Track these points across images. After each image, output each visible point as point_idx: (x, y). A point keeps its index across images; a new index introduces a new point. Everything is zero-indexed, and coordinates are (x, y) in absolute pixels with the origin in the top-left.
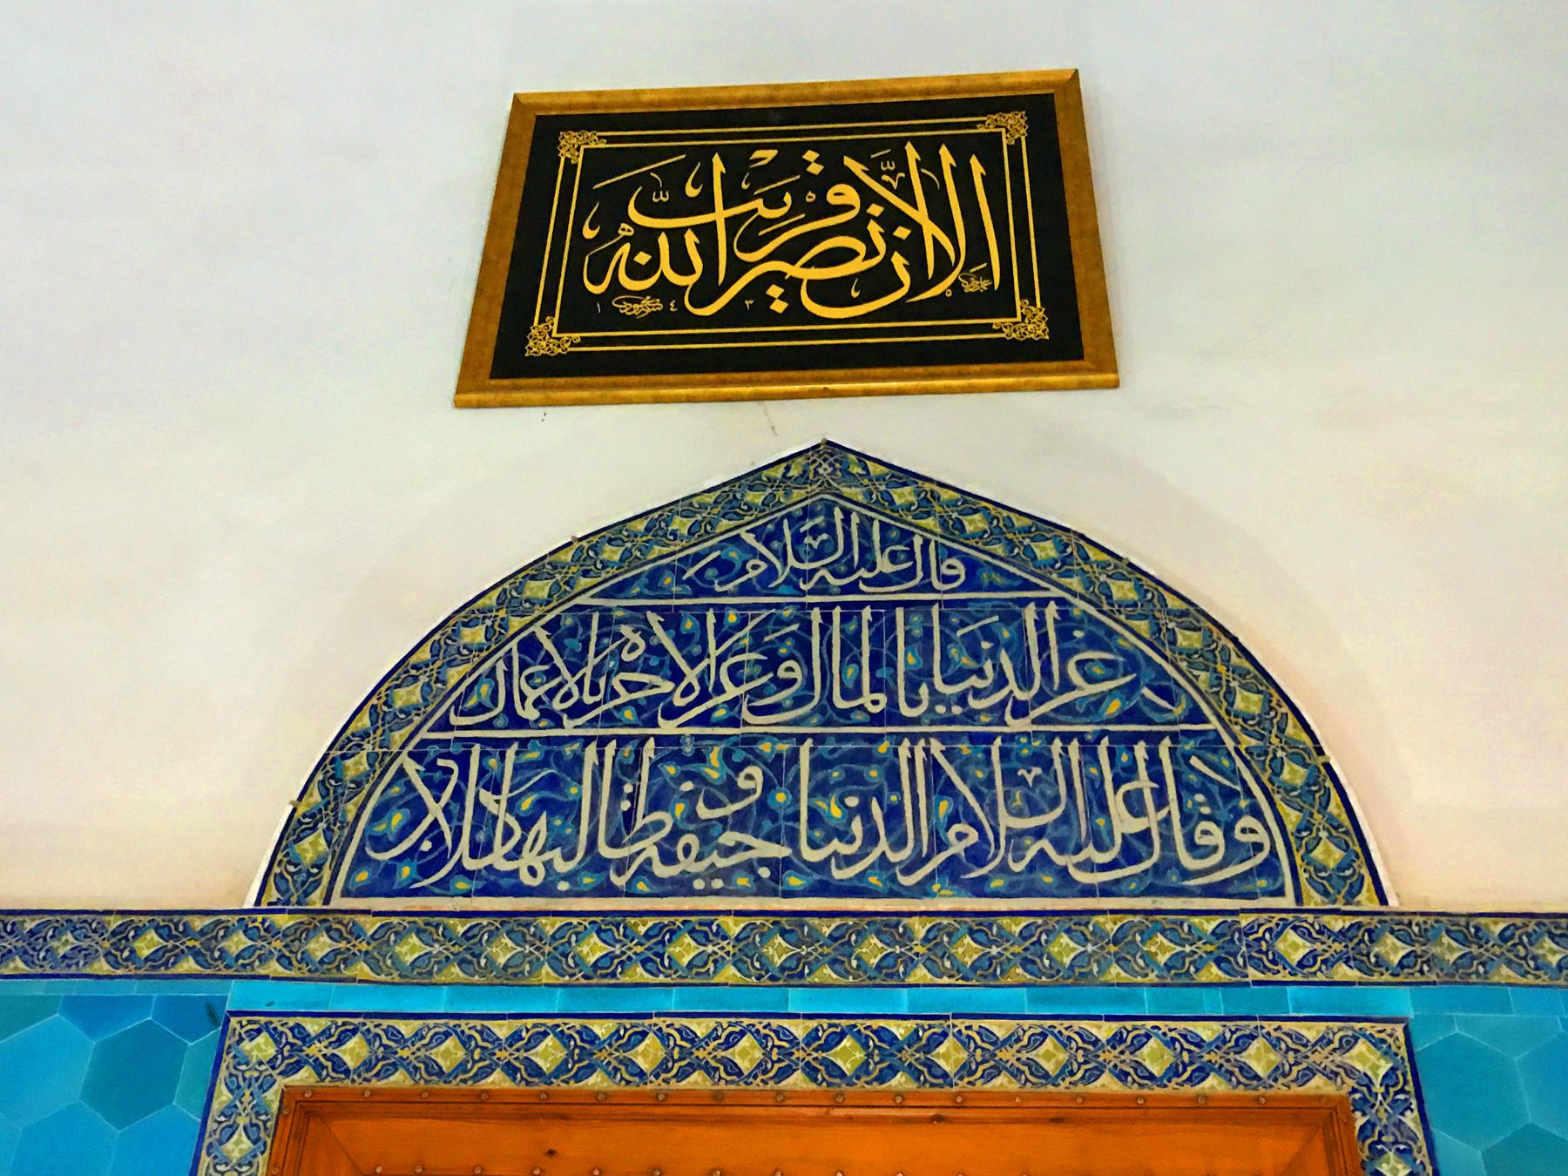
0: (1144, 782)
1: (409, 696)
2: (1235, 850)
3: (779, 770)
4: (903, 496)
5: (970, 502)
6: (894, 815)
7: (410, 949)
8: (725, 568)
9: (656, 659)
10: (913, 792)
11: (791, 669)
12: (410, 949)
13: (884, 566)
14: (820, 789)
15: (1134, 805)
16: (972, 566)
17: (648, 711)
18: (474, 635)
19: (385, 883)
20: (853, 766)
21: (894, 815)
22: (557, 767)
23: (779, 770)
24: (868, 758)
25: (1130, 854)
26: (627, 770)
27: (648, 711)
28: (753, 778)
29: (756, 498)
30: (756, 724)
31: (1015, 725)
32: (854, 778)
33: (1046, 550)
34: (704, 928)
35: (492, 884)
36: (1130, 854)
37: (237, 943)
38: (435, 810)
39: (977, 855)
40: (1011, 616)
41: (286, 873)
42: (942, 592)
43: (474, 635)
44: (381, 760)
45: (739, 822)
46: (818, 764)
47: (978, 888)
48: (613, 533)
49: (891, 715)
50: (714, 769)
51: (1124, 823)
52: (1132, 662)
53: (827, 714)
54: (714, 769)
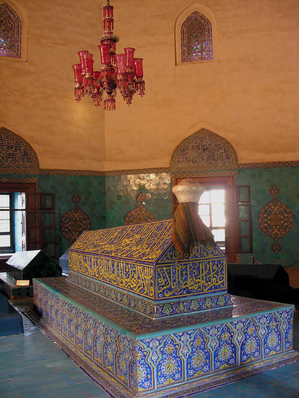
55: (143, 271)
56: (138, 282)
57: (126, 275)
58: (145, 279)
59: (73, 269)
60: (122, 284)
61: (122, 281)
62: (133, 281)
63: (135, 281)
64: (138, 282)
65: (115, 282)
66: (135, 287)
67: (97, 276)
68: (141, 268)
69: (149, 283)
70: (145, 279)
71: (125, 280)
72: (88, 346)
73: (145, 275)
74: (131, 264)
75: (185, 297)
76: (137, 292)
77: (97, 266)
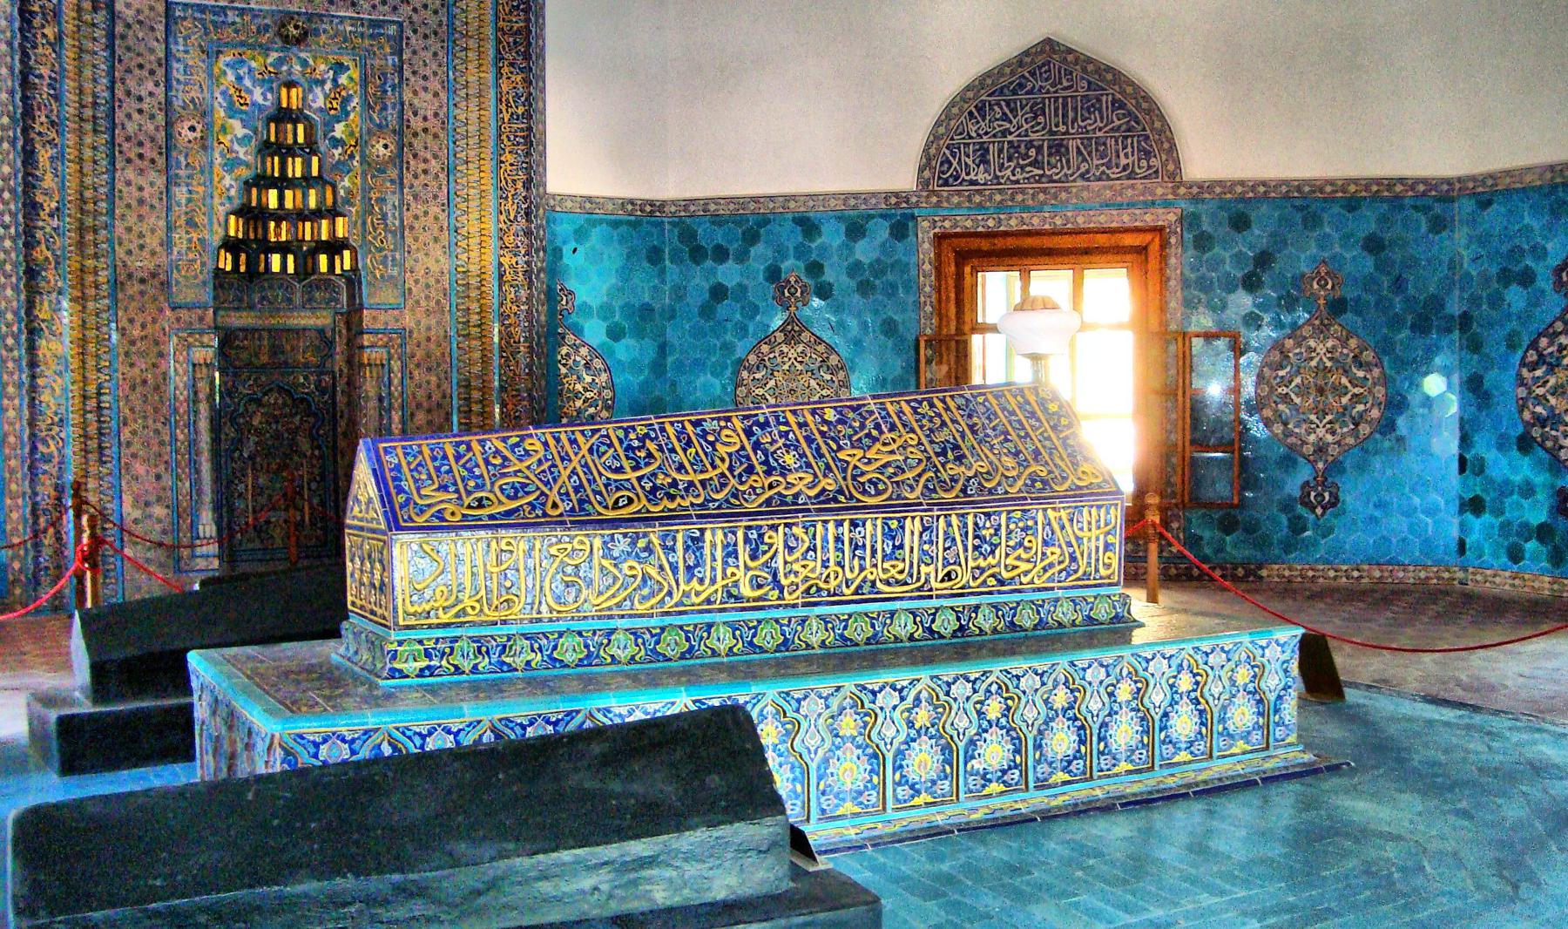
0: (1129, 149)
1: (942, 130)
2: (1149, 167)
3: (1039, 149)
4: (1070, 58)
5: (1090, 60)
6: (1068, 161)
7: (955, 200)
8: (1021, 86)
9: (1005, 118)
10: (1073, 154)
11: (1041, 119)
12: (955, 200)
13: (1065, 84)
14: (1050, 155)
15: (1126, 156)
16: (1089, 83)
17: (1005, 133)
18: (955, 110)
19: (946, 183)
20: (1058, 148)
21: (1068, 161)
22: (983, 151)
23: (1039, 149)
24: (1061, 145)
25: (1124, 169)
26: (1000, 151)
27: (1005, 133)
28: (1032, 152)
29: (1028, 60)
30: (1033, 136)
31: (1099, 134)
32: (1058, 152)
33: (1109, 77)
34: (1023, 191)
35: (972, 183)
36: (1124, 169)
37: (914, 199)
38: (955, 164)
39: (1088, 171)
40: (1099, 100)
41: (924, 183)
42: (1082, 93)
43: (955, 110)
44: (939, 150)
45: (1030, 164)
46: (1049, 147)
47: (1088, 180)
48: (988, 74)
49: (1067, 133)
50: (1023, 150)
51: (1123, 161)
52: (1130, 113)
53: (1051, 133)
54: (1023, 150)
55: (1071, 520)
56: (1044, 554)
57: (976, 548)
58: (1077, 538)
59: (463, 612)
60: (950, 579)
61: (948, 574)
62: (1018, 558)
63: (1024, 556)
64: (1044, 554)
65: (906, 584)
66: (1026, 573)
67: (746, 591)
68: (1063, 514)
69: (1097, 548)
70: (1077, 538)
71: (971, 564)
72: (1050, 764)
73: (1081, 529)
74: (1009, 512)
75: (990, 593)
76: (1038, 583)
77: (754, 557)
